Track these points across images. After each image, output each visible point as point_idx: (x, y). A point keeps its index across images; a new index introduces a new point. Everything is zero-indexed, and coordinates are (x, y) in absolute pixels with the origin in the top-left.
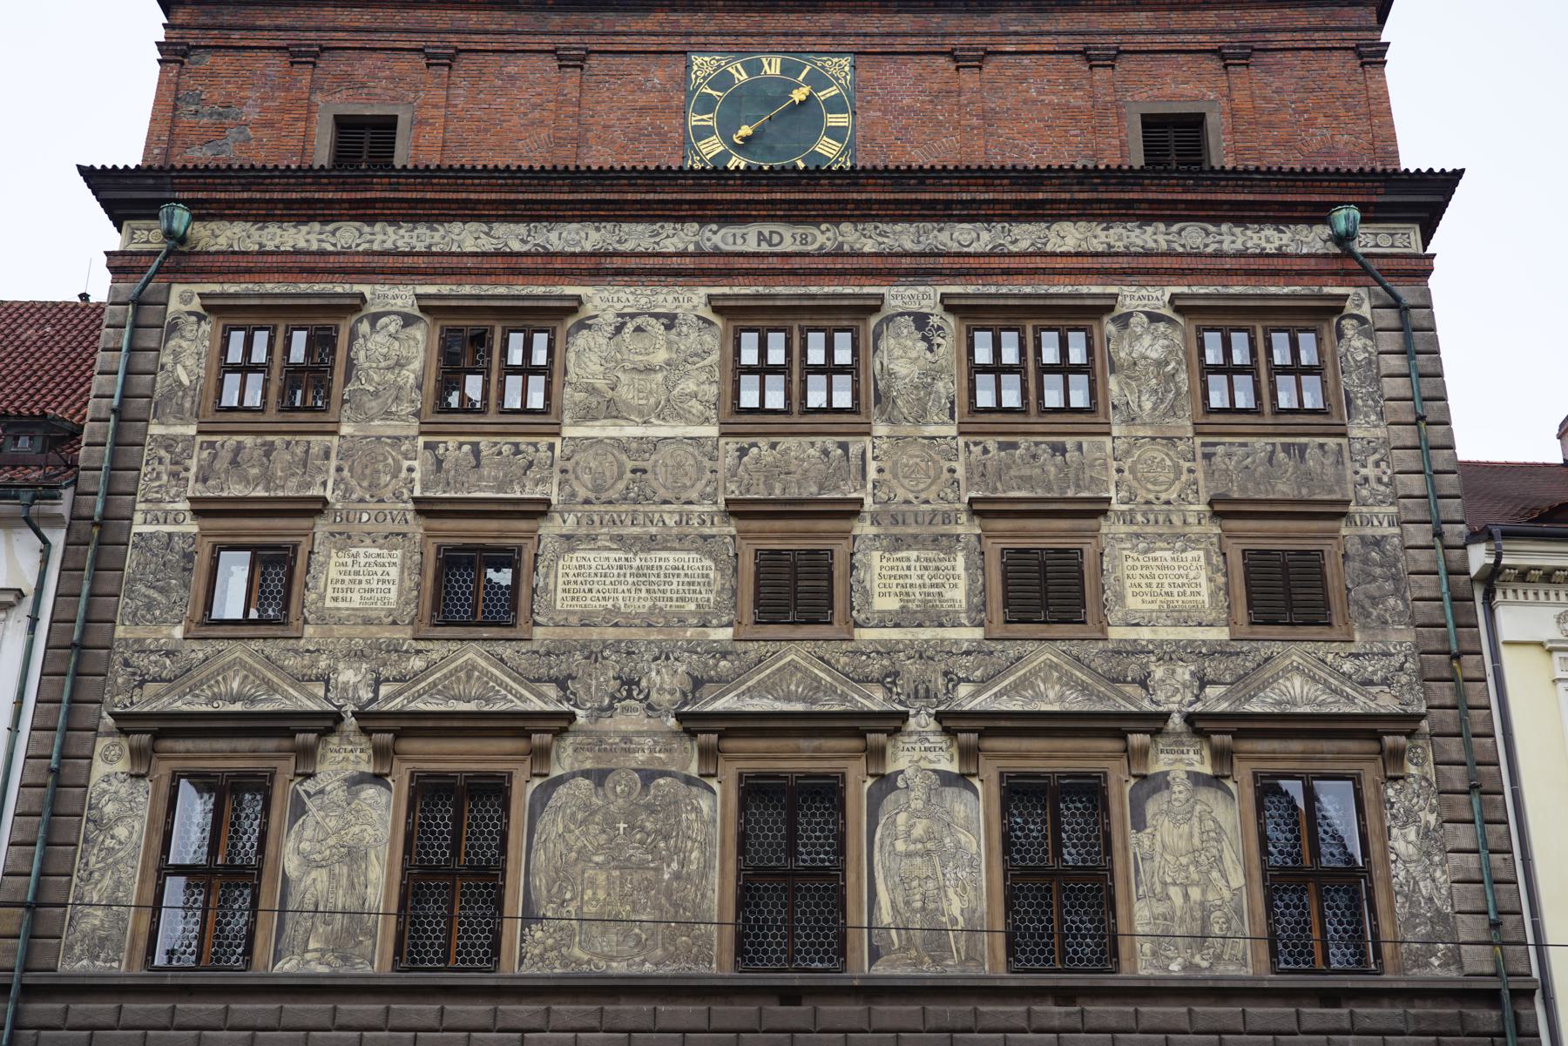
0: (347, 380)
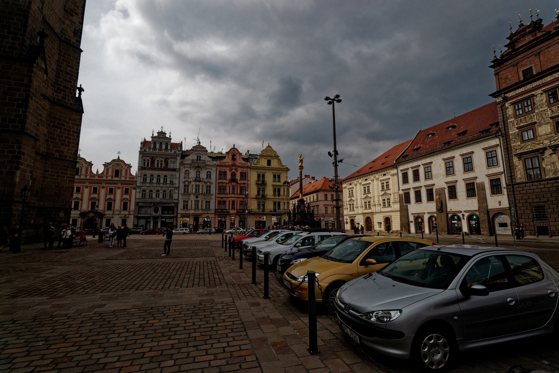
0: (534, 105)
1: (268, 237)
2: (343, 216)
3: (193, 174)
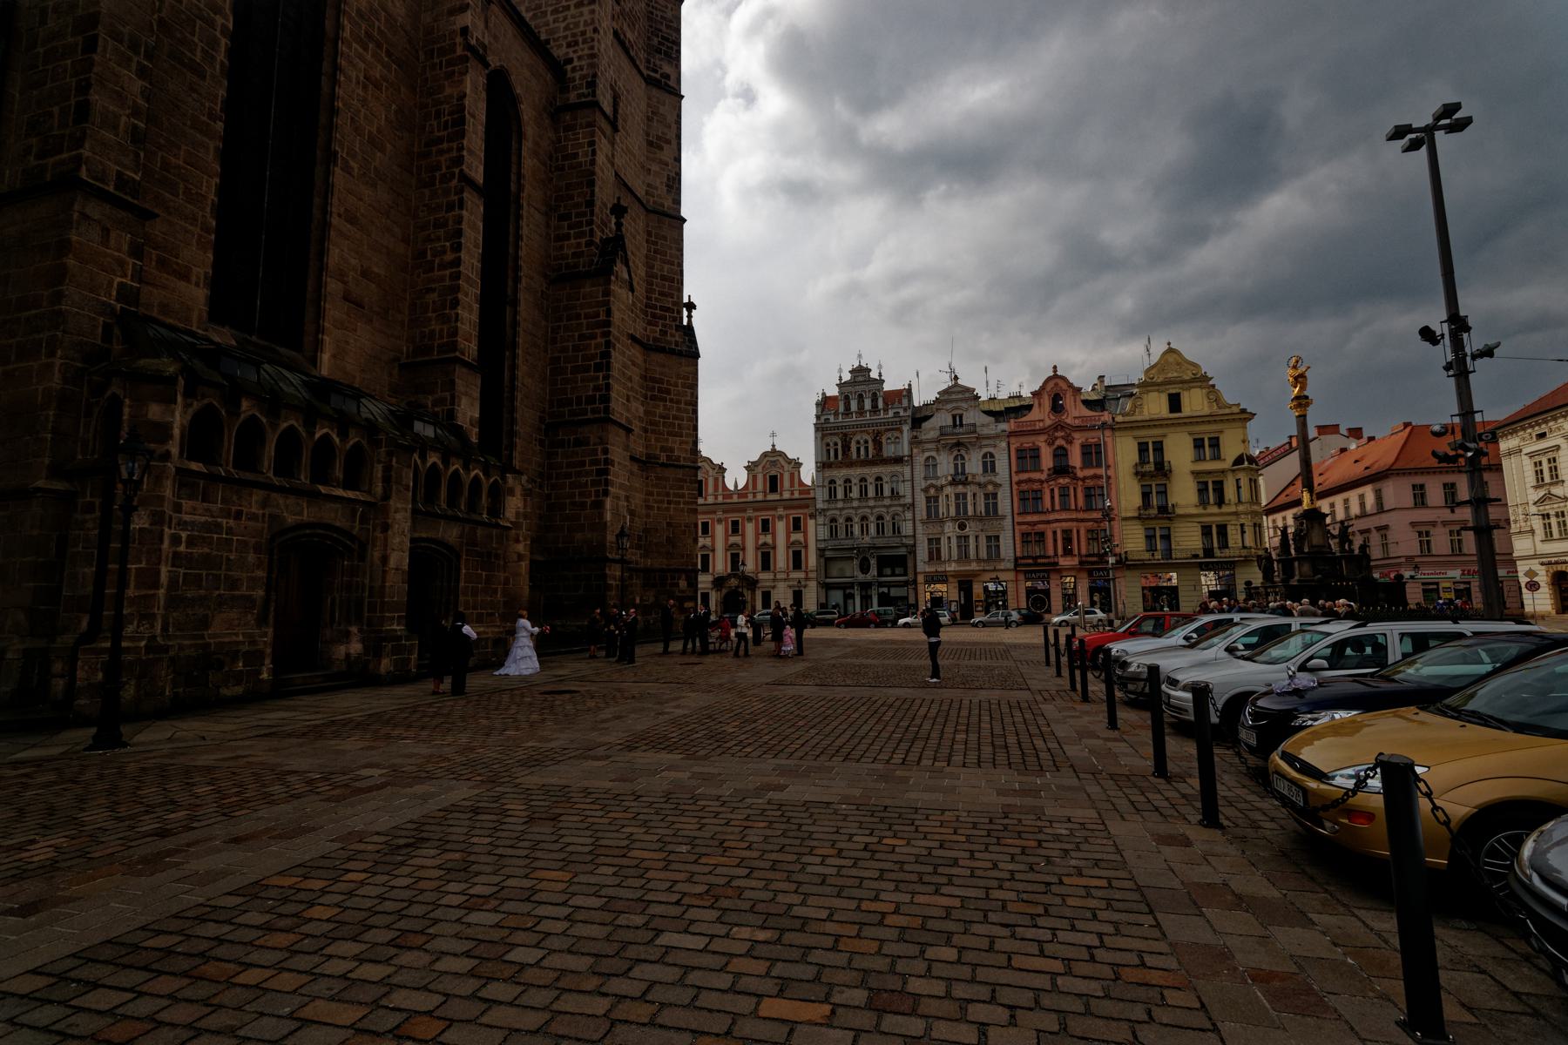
1: (1195, 636)
2: (1511, 562)
3: (945, 465)
